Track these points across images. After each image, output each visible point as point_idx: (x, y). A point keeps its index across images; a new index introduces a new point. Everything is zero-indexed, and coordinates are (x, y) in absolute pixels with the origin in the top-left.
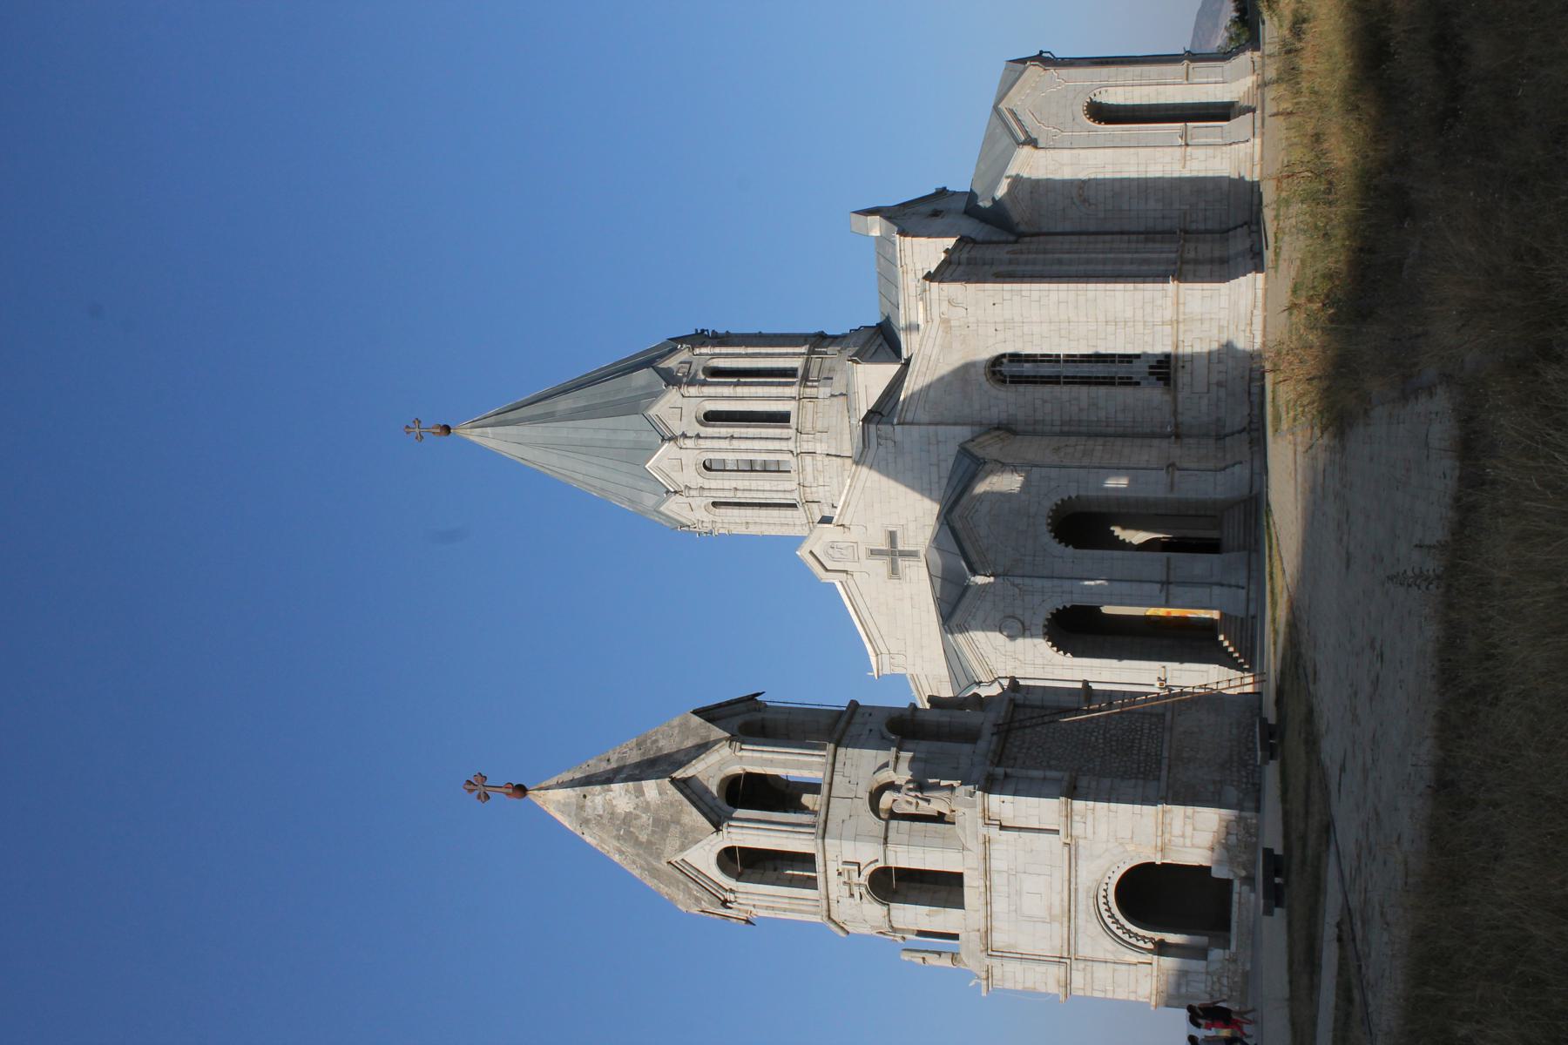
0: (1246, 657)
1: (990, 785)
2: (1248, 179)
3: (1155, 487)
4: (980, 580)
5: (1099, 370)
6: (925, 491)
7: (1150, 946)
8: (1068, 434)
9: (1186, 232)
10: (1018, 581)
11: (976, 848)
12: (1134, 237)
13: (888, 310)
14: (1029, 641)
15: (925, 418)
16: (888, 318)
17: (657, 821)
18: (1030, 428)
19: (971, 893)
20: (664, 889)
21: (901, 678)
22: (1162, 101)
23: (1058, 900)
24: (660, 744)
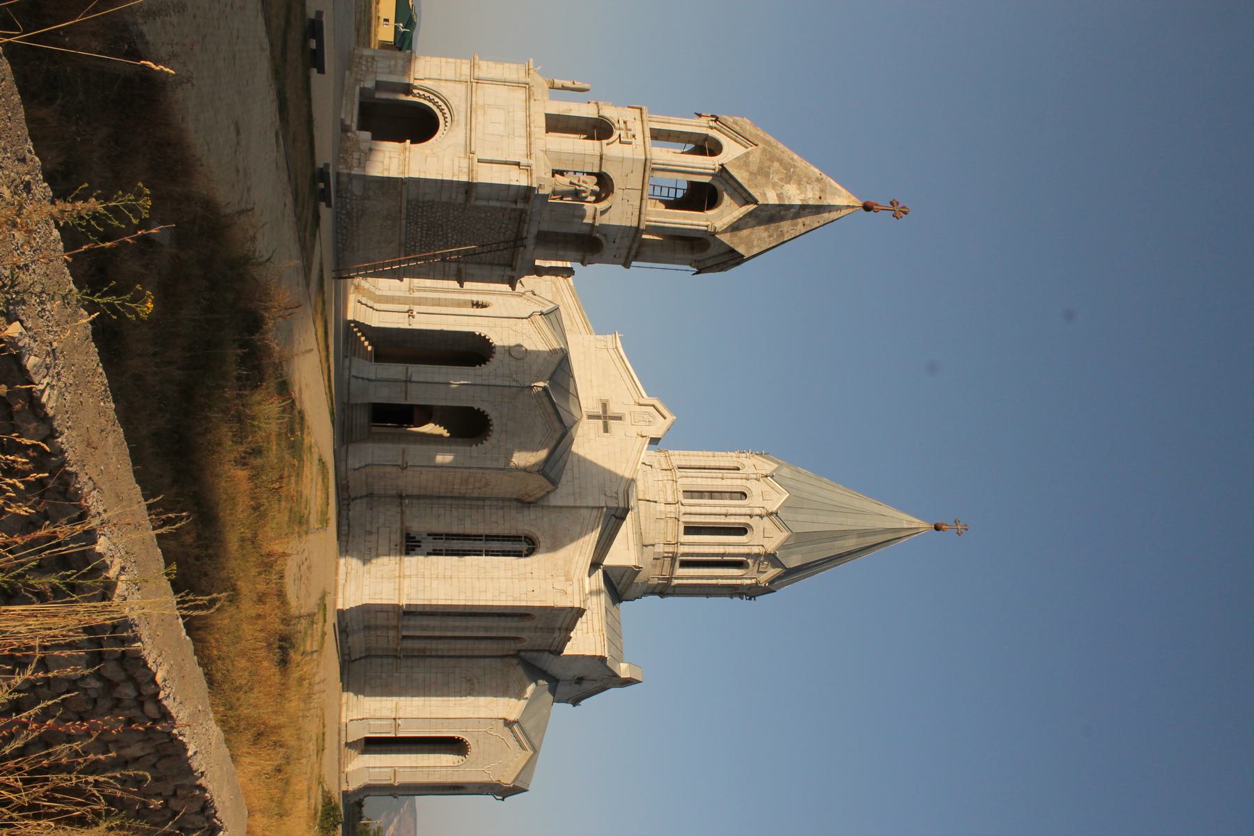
0: (353, 341)
1: (527, 193)
2: (351, 694)
3: (416, 453)
4: (542, 384)
5: (456, 545)
6: (582, 460)
7: (415, 91)
8: (478, 499)
9: (396, 657)
10: (514, 384)
12: (434, 653)
13: (613, 609)
14: (506, 344)
15: (583, 512)
16: (614, 604)
17: (767, 175)
18: (507, 503)
19: (542, 122)
20: (761, 133)
21: (599, 332)
22: (413, 756)
23: (479, 119)
24: (765, 234)
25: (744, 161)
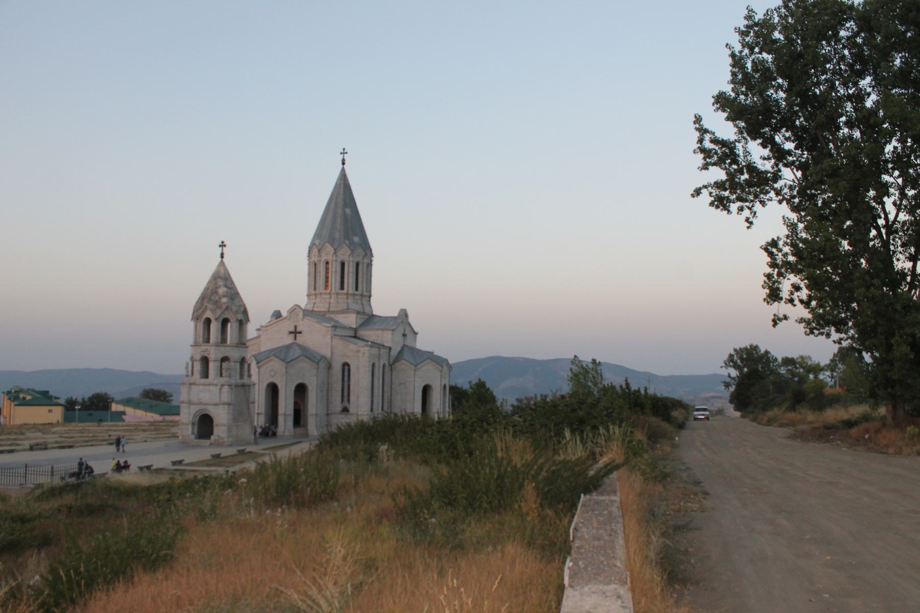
11: (215, 382)
19: (204, 381)
25: (213, 311)
